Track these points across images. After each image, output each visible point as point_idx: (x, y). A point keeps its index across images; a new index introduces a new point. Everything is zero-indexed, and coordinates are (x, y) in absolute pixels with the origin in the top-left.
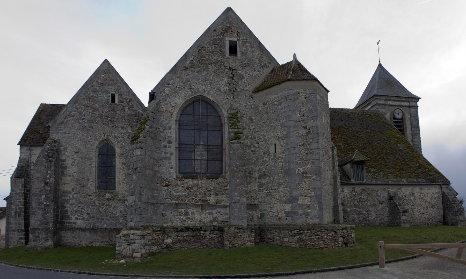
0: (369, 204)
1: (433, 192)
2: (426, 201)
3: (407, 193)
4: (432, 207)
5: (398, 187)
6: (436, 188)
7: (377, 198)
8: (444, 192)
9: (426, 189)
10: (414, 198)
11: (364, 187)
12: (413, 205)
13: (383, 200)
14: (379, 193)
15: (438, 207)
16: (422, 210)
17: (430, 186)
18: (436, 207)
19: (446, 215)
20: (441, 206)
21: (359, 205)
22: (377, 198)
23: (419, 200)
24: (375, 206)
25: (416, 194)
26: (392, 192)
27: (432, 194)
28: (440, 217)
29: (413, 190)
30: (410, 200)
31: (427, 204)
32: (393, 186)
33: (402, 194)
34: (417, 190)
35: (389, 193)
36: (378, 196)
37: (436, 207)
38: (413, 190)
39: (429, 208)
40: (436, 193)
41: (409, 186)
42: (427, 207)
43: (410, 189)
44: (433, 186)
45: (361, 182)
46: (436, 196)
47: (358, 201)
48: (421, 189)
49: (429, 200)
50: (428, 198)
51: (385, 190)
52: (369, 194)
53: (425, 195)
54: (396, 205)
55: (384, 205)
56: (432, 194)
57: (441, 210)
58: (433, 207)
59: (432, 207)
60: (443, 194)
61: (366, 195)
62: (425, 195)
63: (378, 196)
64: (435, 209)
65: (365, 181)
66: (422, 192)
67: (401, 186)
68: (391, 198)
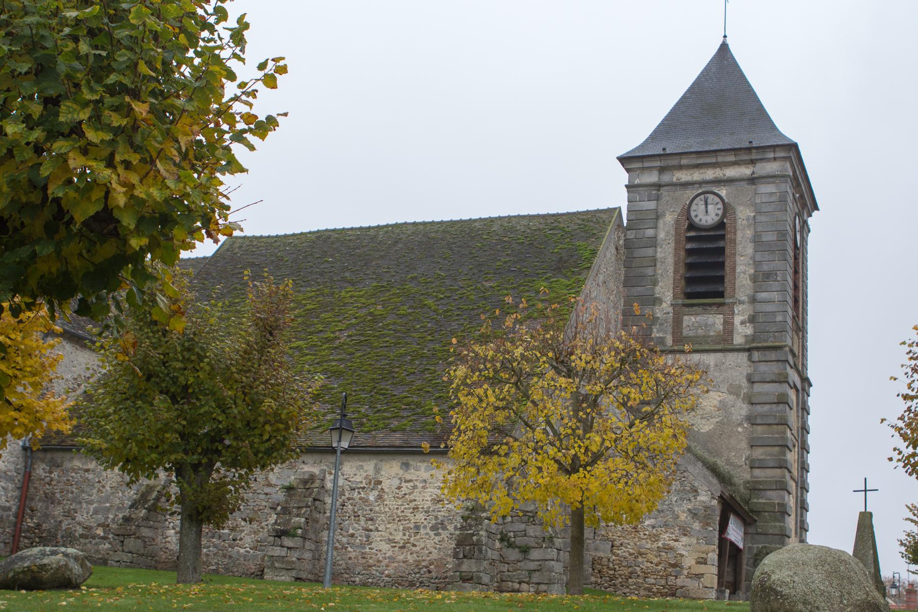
2: (416, 508)
3: (358, 479)
7: (267, 490)
9: (423, 466)
10: (380, 497)
12: (372, 520)
16: (398, 537)
22: (267, 490)
25: (385, 485)
29: (377, 470)
30: (365, 501)
31: (420, 517)
32: (317, 457)
36: (270, 485)
38: (377, 470)
39: (422, 531)
41: (366, 457)
42: (417, 527)
43: (369, 466)
48: (406, 466)
50: (425, 498)
62: (415, 487)
63: (270, 485)
66: (409, 477)
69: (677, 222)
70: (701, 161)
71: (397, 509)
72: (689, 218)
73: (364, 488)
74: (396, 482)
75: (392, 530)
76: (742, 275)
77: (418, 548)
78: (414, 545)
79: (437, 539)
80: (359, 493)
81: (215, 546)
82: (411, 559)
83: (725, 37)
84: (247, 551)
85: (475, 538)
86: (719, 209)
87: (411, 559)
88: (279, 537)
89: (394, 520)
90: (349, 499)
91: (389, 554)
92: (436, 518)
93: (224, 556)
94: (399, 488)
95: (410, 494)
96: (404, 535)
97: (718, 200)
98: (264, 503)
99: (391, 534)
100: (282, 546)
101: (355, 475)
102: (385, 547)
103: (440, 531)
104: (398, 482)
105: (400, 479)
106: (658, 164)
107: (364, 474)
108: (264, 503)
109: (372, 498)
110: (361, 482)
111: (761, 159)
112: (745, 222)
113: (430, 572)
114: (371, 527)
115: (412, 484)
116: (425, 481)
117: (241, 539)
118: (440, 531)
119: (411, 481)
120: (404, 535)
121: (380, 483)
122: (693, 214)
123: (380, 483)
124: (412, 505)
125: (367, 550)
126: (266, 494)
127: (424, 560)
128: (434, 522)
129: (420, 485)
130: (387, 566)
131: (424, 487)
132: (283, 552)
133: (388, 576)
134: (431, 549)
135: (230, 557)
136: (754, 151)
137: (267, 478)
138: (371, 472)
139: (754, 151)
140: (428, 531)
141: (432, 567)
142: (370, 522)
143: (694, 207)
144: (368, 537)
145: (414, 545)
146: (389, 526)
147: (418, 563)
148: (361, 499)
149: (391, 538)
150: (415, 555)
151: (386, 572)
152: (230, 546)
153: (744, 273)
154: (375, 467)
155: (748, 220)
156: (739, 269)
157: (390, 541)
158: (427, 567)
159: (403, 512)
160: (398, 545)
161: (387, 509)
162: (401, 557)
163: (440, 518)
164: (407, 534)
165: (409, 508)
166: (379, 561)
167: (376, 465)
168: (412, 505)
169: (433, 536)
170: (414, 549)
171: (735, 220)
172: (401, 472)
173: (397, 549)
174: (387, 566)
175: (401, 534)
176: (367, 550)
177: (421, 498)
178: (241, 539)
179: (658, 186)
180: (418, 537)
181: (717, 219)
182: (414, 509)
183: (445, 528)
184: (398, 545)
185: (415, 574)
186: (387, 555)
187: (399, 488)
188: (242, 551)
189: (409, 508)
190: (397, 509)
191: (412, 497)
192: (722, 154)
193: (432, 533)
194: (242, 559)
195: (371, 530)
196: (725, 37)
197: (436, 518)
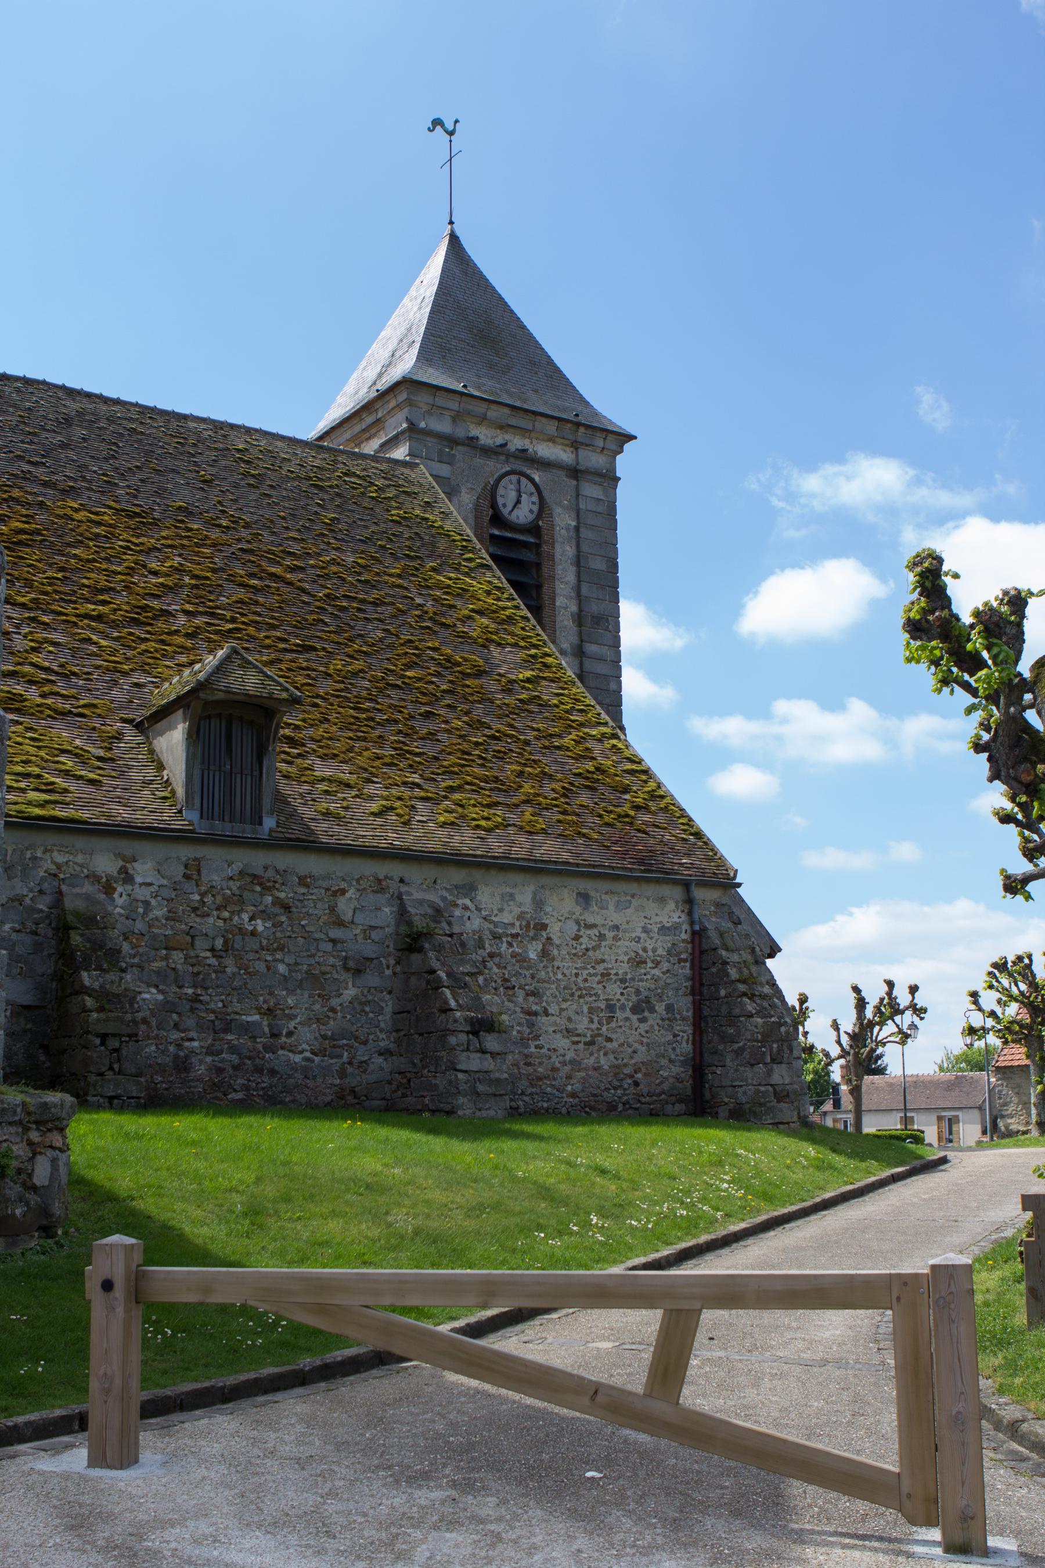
0: (282, 968)
1: (643, 925)
2: (606, 975)
3: (506, 918)
4: (636, 1009)
5: (458, 876)
6: (662, 900)
7: (335, 933)
8: (704, 930)
9: (611, 901)
10: (544, 953)
11: (257, 860)
12: (534, 994)
13: (369, 950)
14: (345, 906)
15: (669, 1008)
16: (582, 1025)
17: (633, 887)
18: (660, 1008)
19: (708, 1058)
20: (685, 1005)
21: (221, 970)
22: (335, 933)
23: (568, 965)
24: (315, 981)
25: (554, 929)
26: (421, 902)
27: (638, 932)
28: (676, 1070)
29: (539, 904)
30: (521, 959)
31: (614, 990)
33: (476, 923)
34: (561, 906)
35: (402, 913)
36: (340, 924)
37: (660, 1008)
38: (539, 904)
39: (619, 1014)
40: (663, 930)
42: (611, 1008)
43: (525, 893)
44: (650, 890)
45: (246, 830)
46: (660, 945)
47: (219, 943)
48: (584, 898)
49: (624, 968)
50: (617, 956)
51: (381, 890)
52: (287, 908)
53: (601, 937)
54: (436, 986)
55: (372, 979)
56: (638, 932)
57: (685, 1030)
58: (642, 1007)
59: (636, 1009)
60: (698, 935)
61: (264, 914)
62: (601, 937)
63: (340, 924)
64: (653, 1020)
65: (269, 822)
66: (591, 919)
67: (477, 874)
68: (413, 942)
69: (477, 506)
70: (513, 422)
71: (577, 975)
72: (494, 505)
73: (517, 935)
74: (572, 928)
75: (571, 1013)
76: (562, 611)
77: (615, 1044)
78: (609, 1040)
79: (643, 1027)
80: (510, 945)
81: (233, 1049)
82: (605, 1063)
83: (451, 223)
84: (307, 1059)
85: (783, 1029)
86: (533, 503)
87: (605, 1063)
88: (476, 1034)
89: (572, 995)
90: (491, 955)
91: (570, 1055)
92: (638, 992)
93: (259, 1070)
94: (577, 938)
95: (594, 949)
96: (592, 1021)
97: (533, 490)
98: (332, 960)
99: (569, 1019)
100: (483, 1051)
101: (501, 910)
102: (562, 1043)
103: (646, 1014)
104: (576, 928)
105: (577, 922)
106: (455, 406)
107: (517, 911)
108: (332, 960)
109: (532, 955)
110: (513, 925)
111: (587, 445)
112: (563, 532)
113: (636, 1084)
114: (534, 1008)
115: (595, 931)
116: (616, 928)
117: (290, 1034)
118: (646, 1014)
119: (594, 926)
120: (592, 1021)
121: (544, 927)
122: (500, 501)
123: (544, 927)
124: (600, 969)
125: (533, 1050)
126: (334, 941)
127: (625, 1065)
128: (634, 998)
129: (610, 935)
130: (569, 1077)
131: (616, 938)
132: (489, 1064)
133: (573, 1095)
134: (636, 1045)
135: (273, 1072)
136: (582, 430)
137: (332, 909)
138: (528, 908)
139: (582, 430)
140: (628, 1013)
141: (639, 1076)
142: (531, 999)
143: (501, 491)
144: (531, 1025)
145: (609, 1040)
146: (564, 1006)
147: (616, 1069)
148: (514, 955)
149: (571, 1026)
150: (611, 1057)
151: (569, 1088)
152: (268, 1048)
153: (566, 608)
154: (534, 898)
155: (567, 529)
156: (560, 601)
157: (569, 1032)
158: (631, 1076)
159: (586, 980)
160: (583, 1039)
161: (560, 976)
162: (591, 1061)
163: (645, 993)
164: (596, 1019)
165: (595, 975)
166: (554, 1069)
167: (535, 894)
168: (600, 969)
169: (636, 1024)
170: (609, 1045)
171: (552, 526)
172: (578, 910)
173: (581, 1046)
174: (569, 1077)
175: (586, 1020)
176: (533, 1050)
177: (613, 958)
178: (290, 1034)
179: (452, 441)
180: (613, 1025)
181: (531, 517)
182: (602, 975)
183: (652, 1010)
184: (583, 1039)
185: (615, 1088)
186: (568, 1058)
187: (577, 938)
188: (297, 1058)
189: (595, 975)
190: (577, 975)
191: (598, 955)
192: (543, 420)
193: (634, 1018)
194: (299, 1076)
195: (536, 1014)
196: (451, 223)
197: (638, 992)
